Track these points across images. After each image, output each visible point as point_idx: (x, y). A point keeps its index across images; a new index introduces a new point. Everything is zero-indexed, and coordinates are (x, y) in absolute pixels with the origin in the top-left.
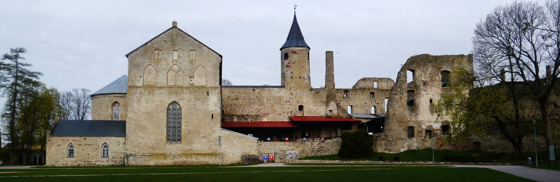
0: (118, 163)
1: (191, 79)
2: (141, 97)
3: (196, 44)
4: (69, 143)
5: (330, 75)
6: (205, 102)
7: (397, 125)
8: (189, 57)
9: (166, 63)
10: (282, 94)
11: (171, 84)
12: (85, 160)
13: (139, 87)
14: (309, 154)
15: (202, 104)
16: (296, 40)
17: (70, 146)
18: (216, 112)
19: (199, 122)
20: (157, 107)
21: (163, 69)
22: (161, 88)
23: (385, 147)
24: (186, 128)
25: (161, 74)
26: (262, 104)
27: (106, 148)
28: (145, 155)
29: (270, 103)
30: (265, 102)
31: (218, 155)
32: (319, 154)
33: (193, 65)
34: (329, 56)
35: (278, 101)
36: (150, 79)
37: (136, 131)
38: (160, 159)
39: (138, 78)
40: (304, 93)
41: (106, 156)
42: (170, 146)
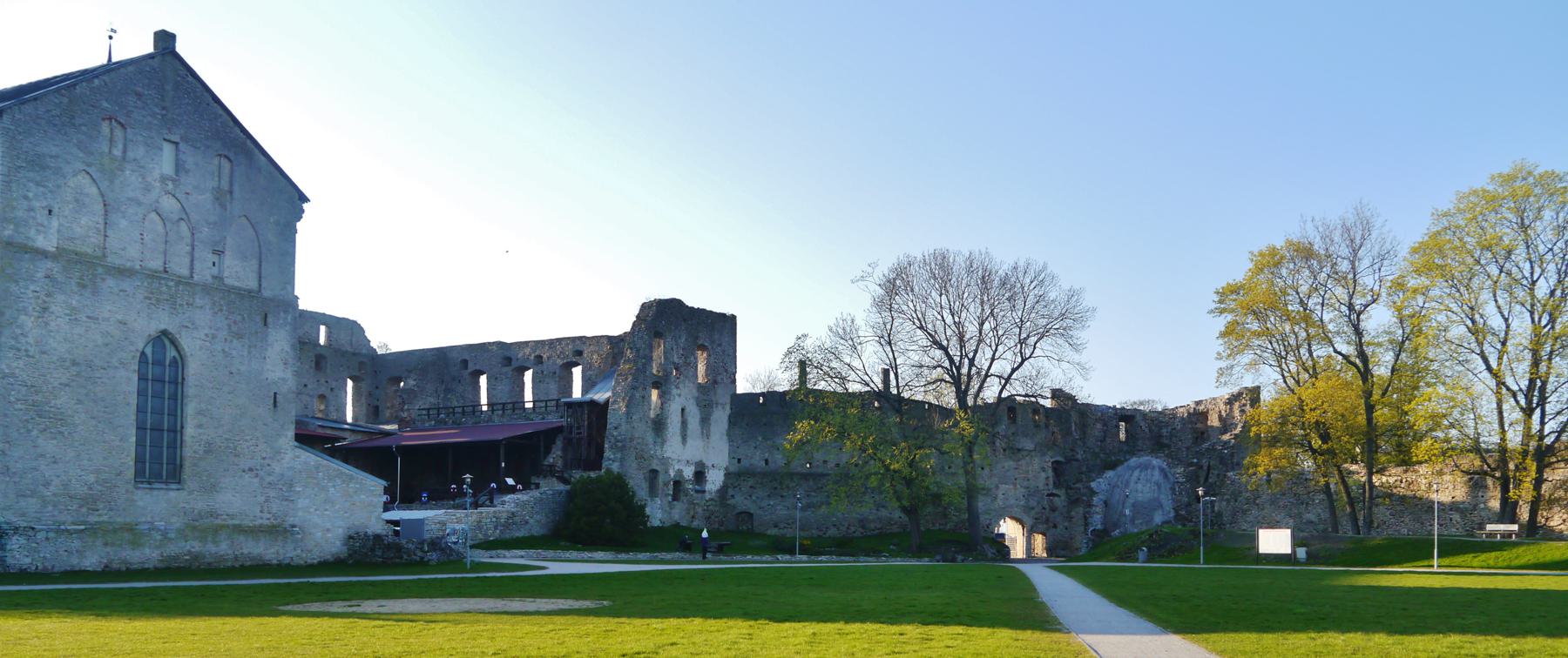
6: (255, 346)
7: (634, 465)
13: (44, 254)
15: (249, 353)
21: (129, 199)
24: (200, 434)
25: (124, 217)
28: (67, 531)
38: (120, 545)
42: (148, 496)
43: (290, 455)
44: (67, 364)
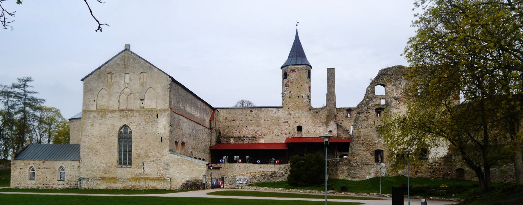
0: (73, 186)
1: (142, 102)
2: (94, 121)
3: (147, 66)
4: (30, 166)
5: (331, 94)
6: (154, 125)
7: (362, 148)
8: (140, 80)
9: (118, 86)
10: (280, 114)
11: (123, 108)
12: (43, 183)
13: (92, 111)
14: (261, 180)
15: (152, 127)
16: (295, 58)
17: (31, 169)
18: (165, 136)
19: (148, 145)
20: (109, 131)
21: (115, 92)
22: (113, 111)
23: (348, 173)
24: (136, 152)
25: (113, 97)
26: (259, 125)
27: (62, 172)
28: (97, 179)
29: (267, 124)
30: (262, 123)
31: (167, 180)
32: (272, 181)
33: (144, 87)
34: (331, 72)
35: (276, 122)
36: (103, 103)
37: (89, 155)
38: (111, 183)
39: (92, 102)
40: (303, 113)
41: (63, 179)
42: (121, 170)
43: (167, 155)
44: (98, 137)
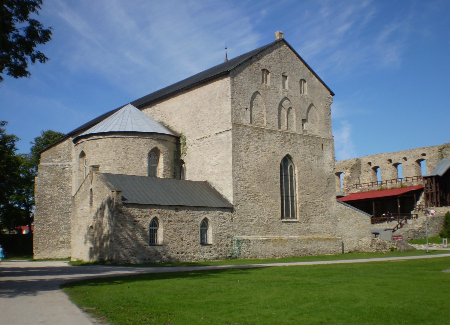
24: (303, 197)
